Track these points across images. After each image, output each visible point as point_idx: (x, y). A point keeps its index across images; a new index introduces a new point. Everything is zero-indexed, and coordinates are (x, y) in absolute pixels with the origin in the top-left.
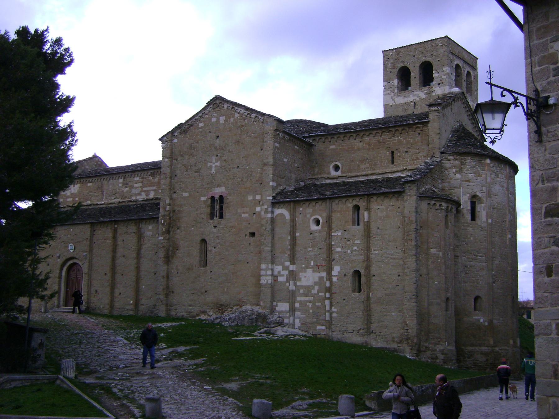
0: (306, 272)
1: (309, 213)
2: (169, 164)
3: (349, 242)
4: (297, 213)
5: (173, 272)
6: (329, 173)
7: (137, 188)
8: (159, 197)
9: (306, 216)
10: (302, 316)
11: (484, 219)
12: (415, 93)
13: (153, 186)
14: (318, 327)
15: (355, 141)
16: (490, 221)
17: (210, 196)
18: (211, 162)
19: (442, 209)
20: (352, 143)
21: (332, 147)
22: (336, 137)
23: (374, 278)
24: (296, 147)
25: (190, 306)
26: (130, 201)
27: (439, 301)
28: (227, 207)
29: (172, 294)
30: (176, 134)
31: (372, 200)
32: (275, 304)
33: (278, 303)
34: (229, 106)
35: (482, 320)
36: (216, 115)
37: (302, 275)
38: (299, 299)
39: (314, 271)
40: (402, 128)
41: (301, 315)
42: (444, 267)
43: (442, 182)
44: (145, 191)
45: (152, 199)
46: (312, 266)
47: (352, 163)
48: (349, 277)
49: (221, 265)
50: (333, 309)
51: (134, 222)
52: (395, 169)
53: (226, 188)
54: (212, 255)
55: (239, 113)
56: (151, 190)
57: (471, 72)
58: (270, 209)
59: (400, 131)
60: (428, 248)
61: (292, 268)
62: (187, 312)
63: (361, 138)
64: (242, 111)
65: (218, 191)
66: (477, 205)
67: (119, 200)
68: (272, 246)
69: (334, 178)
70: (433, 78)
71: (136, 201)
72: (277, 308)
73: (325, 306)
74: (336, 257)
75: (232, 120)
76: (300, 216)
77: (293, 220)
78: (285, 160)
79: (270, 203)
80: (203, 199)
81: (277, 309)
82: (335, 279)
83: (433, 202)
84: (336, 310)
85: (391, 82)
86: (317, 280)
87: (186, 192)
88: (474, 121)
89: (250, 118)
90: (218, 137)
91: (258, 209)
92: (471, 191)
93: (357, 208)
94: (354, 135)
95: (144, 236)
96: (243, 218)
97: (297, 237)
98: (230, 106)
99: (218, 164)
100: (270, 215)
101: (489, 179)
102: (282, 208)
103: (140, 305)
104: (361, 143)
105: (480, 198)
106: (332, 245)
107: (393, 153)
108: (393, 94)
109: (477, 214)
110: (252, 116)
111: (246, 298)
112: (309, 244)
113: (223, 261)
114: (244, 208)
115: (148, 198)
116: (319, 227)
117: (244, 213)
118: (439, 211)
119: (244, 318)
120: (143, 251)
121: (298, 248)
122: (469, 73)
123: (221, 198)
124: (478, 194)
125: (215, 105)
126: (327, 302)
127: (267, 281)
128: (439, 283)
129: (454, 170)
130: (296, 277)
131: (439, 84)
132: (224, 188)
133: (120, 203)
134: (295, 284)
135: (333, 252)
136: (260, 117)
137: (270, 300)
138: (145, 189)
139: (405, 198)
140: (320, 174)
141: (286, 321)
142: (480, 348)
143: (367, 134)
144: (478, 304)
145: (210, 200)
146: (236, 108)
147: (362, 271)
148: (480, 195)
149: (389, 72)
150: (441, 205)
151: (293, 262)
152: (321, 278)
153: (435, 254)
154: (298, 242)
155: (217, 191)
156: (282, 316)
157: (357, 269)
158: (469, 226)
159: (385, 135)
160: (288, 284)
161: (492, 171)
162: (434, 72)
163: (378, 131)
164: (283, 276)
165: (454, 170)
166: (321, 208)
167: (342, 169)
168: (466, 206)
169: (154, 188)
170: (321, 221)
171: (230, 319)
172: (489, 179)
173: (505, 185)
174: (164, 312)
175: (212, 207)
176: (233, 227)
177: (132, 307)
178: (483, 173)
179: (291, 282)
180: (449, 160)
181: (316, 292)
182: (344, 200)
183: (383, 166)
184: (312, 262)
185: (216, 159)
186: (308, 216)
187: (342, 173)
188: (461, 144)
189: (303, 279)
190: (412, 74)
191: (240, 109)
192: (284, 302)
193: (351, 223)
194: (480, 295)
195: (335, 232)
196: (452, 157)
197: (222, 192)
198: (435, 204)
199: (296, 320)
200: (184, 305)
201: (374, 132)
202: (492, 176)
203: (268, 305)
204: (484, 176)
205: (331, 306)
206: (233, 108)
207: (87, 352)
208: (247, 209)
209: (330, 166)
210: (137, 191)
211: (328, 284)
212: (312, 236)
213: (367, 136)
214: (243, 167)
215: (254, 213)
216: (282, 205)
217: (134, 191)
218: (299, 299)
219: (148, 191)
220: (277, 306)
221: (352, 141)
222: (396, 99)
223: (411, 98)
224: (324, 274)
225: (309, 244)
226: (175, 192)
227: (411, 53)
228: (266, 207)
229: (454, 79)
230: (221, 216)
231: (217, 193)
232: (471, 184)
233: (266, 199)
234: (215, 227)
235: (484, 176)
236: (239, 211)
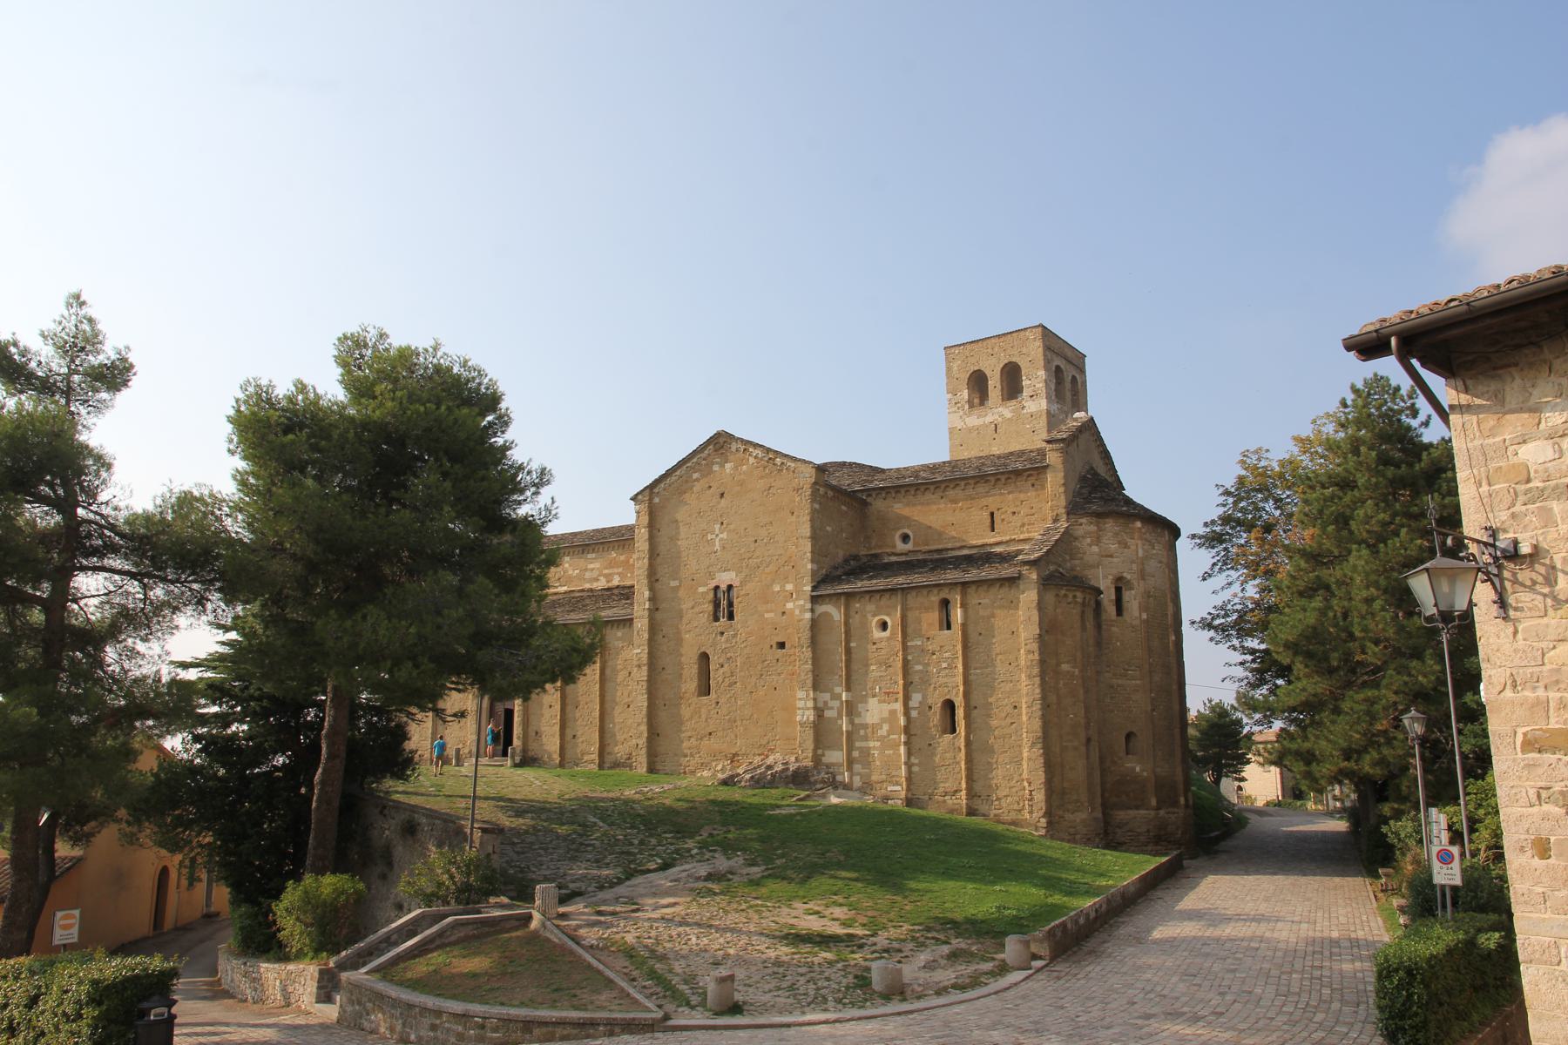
3: (934, 657)
4: (852, 613)
6: (895, 547)
7: (592, 570)
8: (628, 583)
11: (1136, 613)
13: (618, 567)
14: (889, 789)
16: (1144, 616)
18: (713, 533)
19: (1076, 603)
22: (903, 491)
23: (976, 711)
24: (844, 508)
26: (583, 591)
27: (1076, 743)
30: (656, 490)
31: (969, 590)
32: (820, 752)
35: (1138, 769)
36: (718, 460)
38: (858, 744)
39: (880, 702)
40: (1007, 476)
42: (1081, 692)
43: (1072, 559)
44: (606, 576)
45: (618, 587)
48: (937, 707)
50: (914, 760)
52: (998, 539)
53: (739, 572)
55: (756, 457)
57: (1078, 377)
58: (809, 606)
59: (1003, 480)
60: (1058, 664)
65: (724, 579)
66: (1123, 592)
67: (565, 589)
68: (813, 664)
69: (901, 554)
71: (591, 590)
72: (823, 758)
73: (900, 755)
74: (916, 679)
77: (847, 623)
78: (829, 529)
79: (809, 598)
80: (701, 589)
81: (825, 760)
82: (914, 714)
83: (1063, 592)
84: (916, 761)
86: (886, 714)
87: (674, 580)
90: (722, 495)
91: (790, 605)
92: (1114, 571)
93: (945, 604)
94: (932, 487)
99: (724, 535)
100: (808, 616)
101: (1141, 553)
105: (1129, 581)
106: (908, 661)
107: (992, 514)
108: (961, 413)
109: (1125, 605)
115: (610, 585)
116: (887, 633)
117: (768, 612)
118: (1072, 605)
122: (1074, 378)
123: (730, 587)
124: (1125, 575)
125: (717, 446)
126: (902, 749)
128: (1075, 715)
129: (1089, 540)
131: (1032, 396)
133: (566, 593)
134: (851, 722)
135: (910, 671)
137: (812, 747)
138: (606, 571)
139: (1021, 587)
140: (880, 547)
141: (839, 778)
142: (1136, 812)
144: (1131, 744)
145: (712, 592)
146: (751, 450)
147: (959, 701)
148: (1129, 577)
150: (1075, 597)
151: (848, 689)
152: (893, 713)
153: (1068, 672)
154: (854, 656)
157: (948, 697)
158: (1113, 626)
161: (1146, 540)
162: (1024, 378)
164: (832, 708)
165: (1089, 540)
167: (914, 539)
168: (1108, 597)
169: (620, 570)
170: (889, 624)
171: (752, 777)
172: (1141, 553)
173: (1165, 560)
175: (717, 604)
177: (595, 757)
178: (1131, 542)
180: (1081, 525)
181: (885, 734)
182: (925, 592)
187: (915, 544)
188: (1095, 498)
193: (937, 626)
194: (1134, 730)
195: (912, 640)
196: (1084, 520)
198: (1065, 596)
199: (854, 778)
201: (963, 483)
202: (1145, 547)
203: (810, 755)
204: (1133, 547)
205: (909, 754)
206: (745, 450)
207: (551, 850)
209: (895, 536)
210: (595, 574)
211: (902, 721)
215: (784, 613)
216: (827, 600)
217: (588, 575)
219: (610, 574)
220: (823, 755)
222: (967, 420)
223: (989, 419)
224: (899, 706)
228: (802, 602)
230: (731, 617)
232: (1115, 560)
235: (1133, 547)
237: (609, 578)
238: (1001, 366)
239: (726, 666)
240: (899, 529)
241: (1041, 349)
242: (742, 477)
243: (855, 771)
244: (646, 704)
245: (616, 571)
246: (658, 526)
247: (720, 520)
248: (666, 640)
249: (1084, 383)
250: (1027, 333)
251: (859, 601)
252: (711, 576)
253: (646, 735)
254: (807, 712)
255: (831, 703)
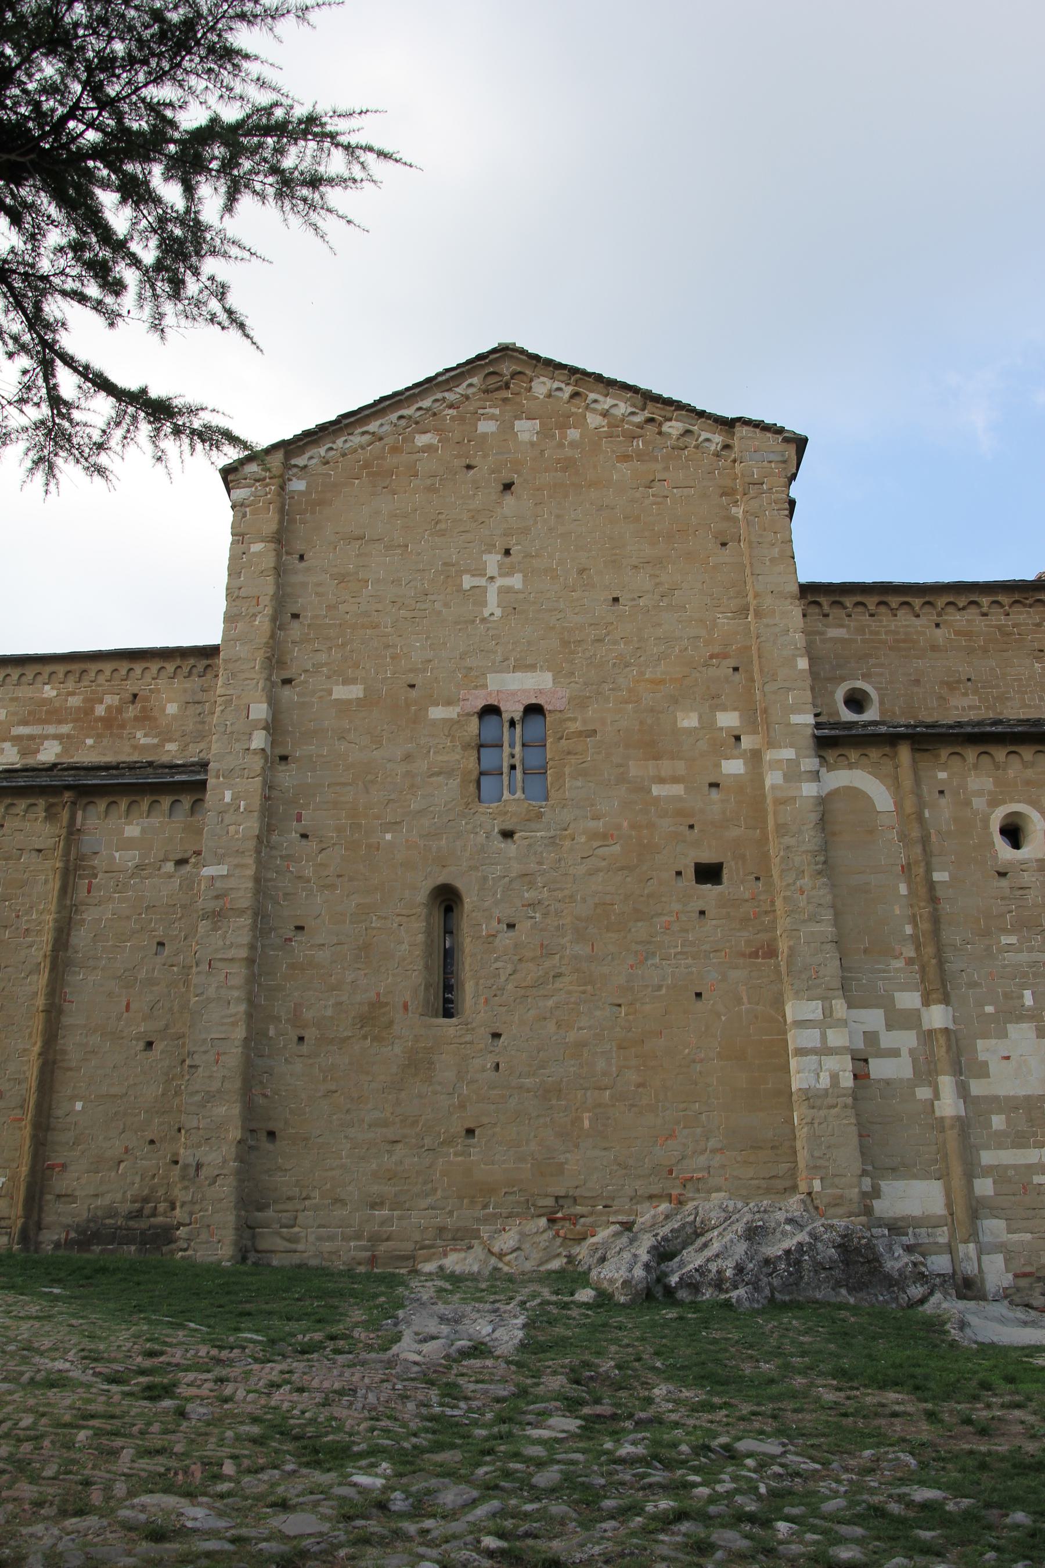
0: (1004, 1035)
1: (980, 793)
2: (269, 561)
5: (272, 1033)
9: (968, 803)
10: (1015, 1237)
13: (60, 722)
15: (917, 622)
17: (480, 704)
20: (907, 626)
21: (833, 633)
25: (373, 1206)
28: (569, 753)
29: (270, 1146)
30: (301, 461)
33: (882, 1183)
34: (559, 389)
37: (986, 1049)
41: (1010, 1231)
46: (1029, 1009)
47: (916, 689)
49: (550, 1003)
51: (42, 803)
54: (497, 960)
55: (605, 414)
56: (46, 737)
61: (937, 1017)
62: (358, 1237)
63: (939, 615)
64: (622, 408)
75: (573, 434)
76: (943, 801)
87: (346, 682)
89: (660, 433)
95: (94, 868)
96: (657, 799)
97: (938, 887)
98: (563, 386)
100: (809, 789)
102: (850, 766)
103: (48, 1197)
104: (938, 631)
110: (665, 428)
111: (702, 1160)
112: (1002, 915)
113: (557, 985)
114: (657, 758)
115: (30, 761)
117: (662, 781)
119: (798, 1262)
120: (81, 938)
121: (951, 935)
125: (492, 380)
127: (835, 1077)
130: (963, 1060)
132: (548, 676)
134: (963, 1091)
136: (704, 435)
143: (961, 605)
146: (592, 396)
154: (945, 907)
155: (514, 687)
156: (912, 1242)
159: (1021, 613)
160: (923, 1093)
163: (1000, 598)
164: (895, 1053)
166: (1029, 773)
167: (882, 703)
169: (65, 729)
174: (229, 1235)
176: (605, 836)
179: (946, 1083)
183: (1030, 707)
184: (1028, 994)
185: (500, 566)
186: (979, 803)
189: (995, 1067)
191: (610, 401)
192: (915, 1177)
197: (541, 691)
200: (339, 1201)
206: (575, 395)
208: (666, 767)
209: (833, 693)
212: (1004, 883)
213: (959, 609)
214: (641, 602)
215: (714, 785)
216: (853, 755)
218: (987, 1157)
219: (31, 738)
221: (904, 618)
225: (1002, 915)
226: (287, 682)
228: (789, 753)
231: (513, 694)
233: (789, 724)
234: (507, 835)
236: (634, 770)
237: (28, 745)
239: (524, 926)
240: (843, 679)
242: (568, 452)
243: (986, 1238)
244: (240, 1033)
245: (51, 729)
246: (300, 546)
247: (500, 544)
248: (313, 845)
251: (945, 767)
252: (474, 679)
253: (235, 1133)
254: (831, 1063)
255: (888, 1040)
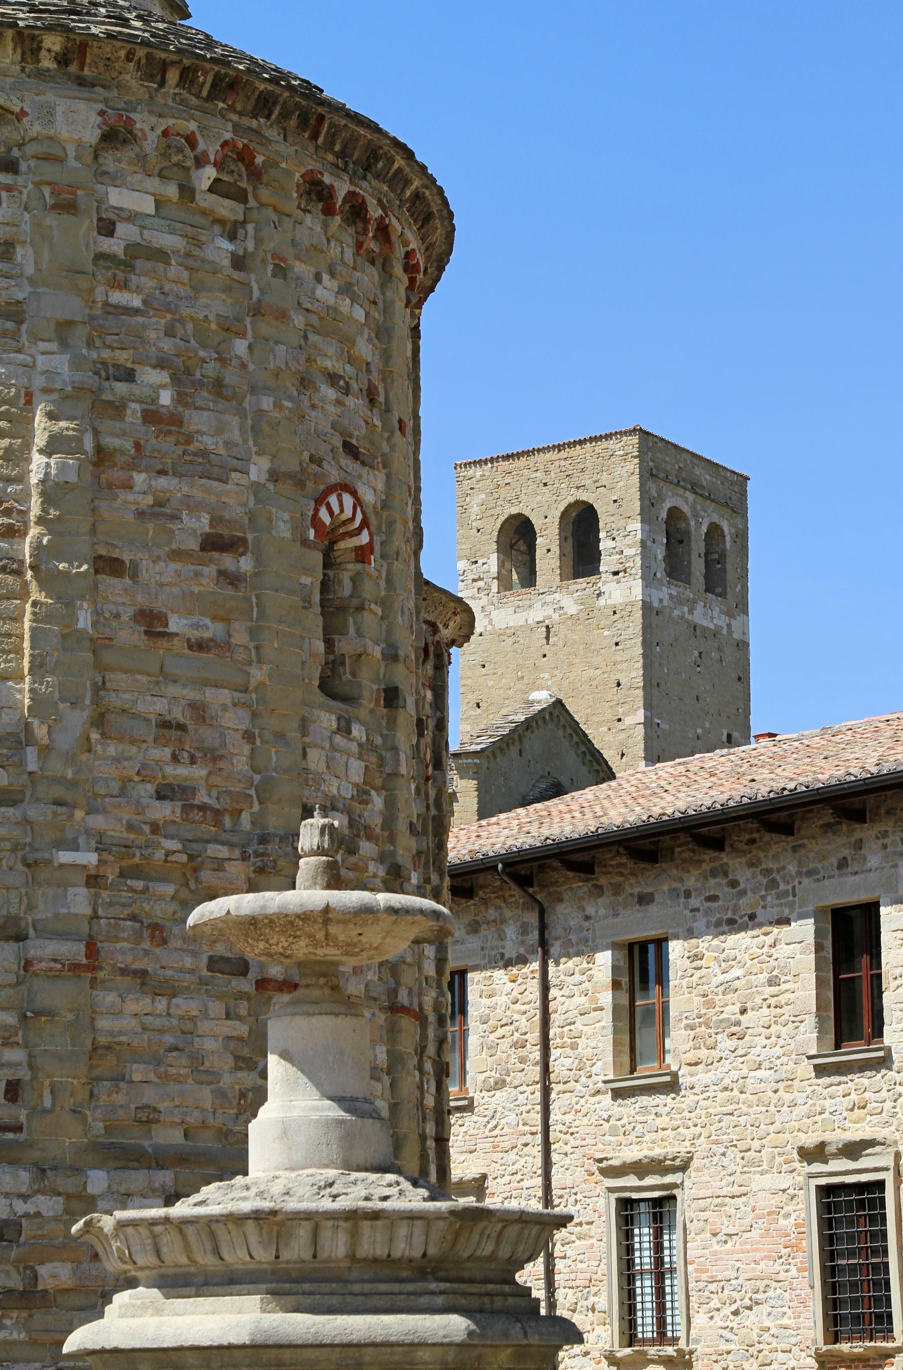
12: (548, 598)
70: (599, 553)
85: (480, 562)
88: (599, 764)
122: (714, 531)
131: (616, 573)
149: (475, 531)
162: (602, 535)
190: (539, 540)
222: (494, 614)
223: (537, 613)
227: (538, 474)
229: (660, 557)
238: (562, 507)
241: (636, 479)
249: (742, 536)
250: (611, 444)
